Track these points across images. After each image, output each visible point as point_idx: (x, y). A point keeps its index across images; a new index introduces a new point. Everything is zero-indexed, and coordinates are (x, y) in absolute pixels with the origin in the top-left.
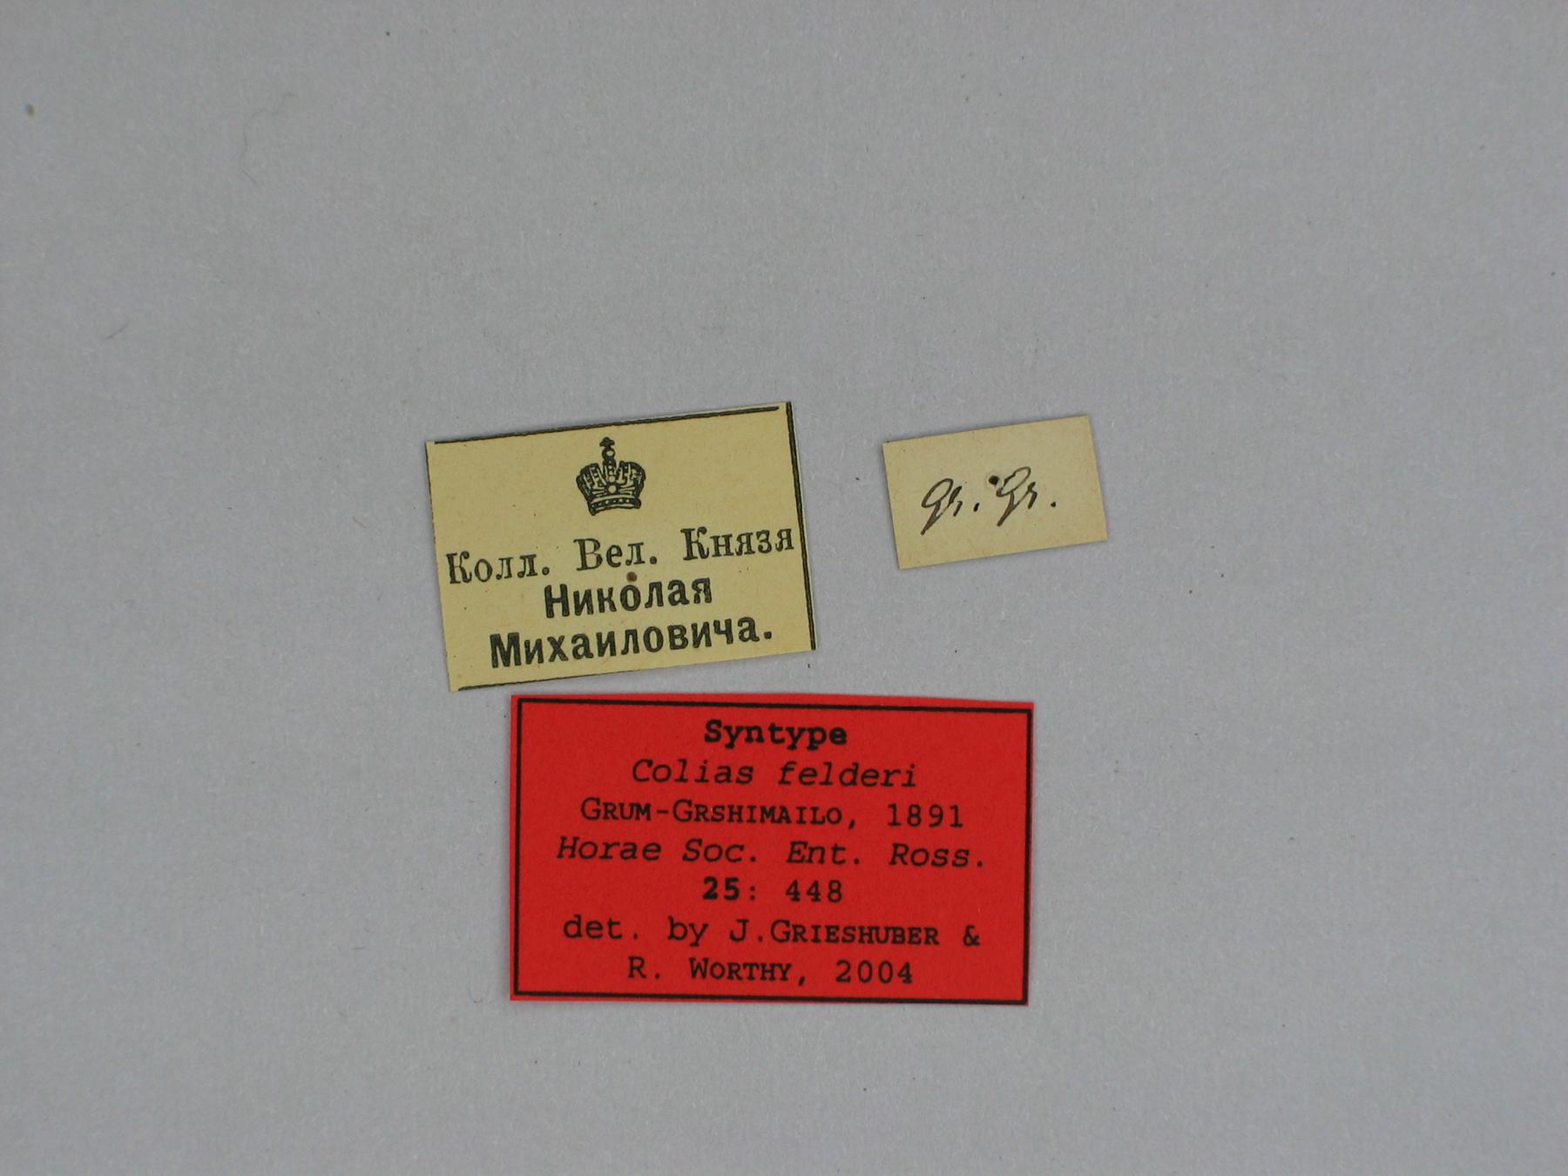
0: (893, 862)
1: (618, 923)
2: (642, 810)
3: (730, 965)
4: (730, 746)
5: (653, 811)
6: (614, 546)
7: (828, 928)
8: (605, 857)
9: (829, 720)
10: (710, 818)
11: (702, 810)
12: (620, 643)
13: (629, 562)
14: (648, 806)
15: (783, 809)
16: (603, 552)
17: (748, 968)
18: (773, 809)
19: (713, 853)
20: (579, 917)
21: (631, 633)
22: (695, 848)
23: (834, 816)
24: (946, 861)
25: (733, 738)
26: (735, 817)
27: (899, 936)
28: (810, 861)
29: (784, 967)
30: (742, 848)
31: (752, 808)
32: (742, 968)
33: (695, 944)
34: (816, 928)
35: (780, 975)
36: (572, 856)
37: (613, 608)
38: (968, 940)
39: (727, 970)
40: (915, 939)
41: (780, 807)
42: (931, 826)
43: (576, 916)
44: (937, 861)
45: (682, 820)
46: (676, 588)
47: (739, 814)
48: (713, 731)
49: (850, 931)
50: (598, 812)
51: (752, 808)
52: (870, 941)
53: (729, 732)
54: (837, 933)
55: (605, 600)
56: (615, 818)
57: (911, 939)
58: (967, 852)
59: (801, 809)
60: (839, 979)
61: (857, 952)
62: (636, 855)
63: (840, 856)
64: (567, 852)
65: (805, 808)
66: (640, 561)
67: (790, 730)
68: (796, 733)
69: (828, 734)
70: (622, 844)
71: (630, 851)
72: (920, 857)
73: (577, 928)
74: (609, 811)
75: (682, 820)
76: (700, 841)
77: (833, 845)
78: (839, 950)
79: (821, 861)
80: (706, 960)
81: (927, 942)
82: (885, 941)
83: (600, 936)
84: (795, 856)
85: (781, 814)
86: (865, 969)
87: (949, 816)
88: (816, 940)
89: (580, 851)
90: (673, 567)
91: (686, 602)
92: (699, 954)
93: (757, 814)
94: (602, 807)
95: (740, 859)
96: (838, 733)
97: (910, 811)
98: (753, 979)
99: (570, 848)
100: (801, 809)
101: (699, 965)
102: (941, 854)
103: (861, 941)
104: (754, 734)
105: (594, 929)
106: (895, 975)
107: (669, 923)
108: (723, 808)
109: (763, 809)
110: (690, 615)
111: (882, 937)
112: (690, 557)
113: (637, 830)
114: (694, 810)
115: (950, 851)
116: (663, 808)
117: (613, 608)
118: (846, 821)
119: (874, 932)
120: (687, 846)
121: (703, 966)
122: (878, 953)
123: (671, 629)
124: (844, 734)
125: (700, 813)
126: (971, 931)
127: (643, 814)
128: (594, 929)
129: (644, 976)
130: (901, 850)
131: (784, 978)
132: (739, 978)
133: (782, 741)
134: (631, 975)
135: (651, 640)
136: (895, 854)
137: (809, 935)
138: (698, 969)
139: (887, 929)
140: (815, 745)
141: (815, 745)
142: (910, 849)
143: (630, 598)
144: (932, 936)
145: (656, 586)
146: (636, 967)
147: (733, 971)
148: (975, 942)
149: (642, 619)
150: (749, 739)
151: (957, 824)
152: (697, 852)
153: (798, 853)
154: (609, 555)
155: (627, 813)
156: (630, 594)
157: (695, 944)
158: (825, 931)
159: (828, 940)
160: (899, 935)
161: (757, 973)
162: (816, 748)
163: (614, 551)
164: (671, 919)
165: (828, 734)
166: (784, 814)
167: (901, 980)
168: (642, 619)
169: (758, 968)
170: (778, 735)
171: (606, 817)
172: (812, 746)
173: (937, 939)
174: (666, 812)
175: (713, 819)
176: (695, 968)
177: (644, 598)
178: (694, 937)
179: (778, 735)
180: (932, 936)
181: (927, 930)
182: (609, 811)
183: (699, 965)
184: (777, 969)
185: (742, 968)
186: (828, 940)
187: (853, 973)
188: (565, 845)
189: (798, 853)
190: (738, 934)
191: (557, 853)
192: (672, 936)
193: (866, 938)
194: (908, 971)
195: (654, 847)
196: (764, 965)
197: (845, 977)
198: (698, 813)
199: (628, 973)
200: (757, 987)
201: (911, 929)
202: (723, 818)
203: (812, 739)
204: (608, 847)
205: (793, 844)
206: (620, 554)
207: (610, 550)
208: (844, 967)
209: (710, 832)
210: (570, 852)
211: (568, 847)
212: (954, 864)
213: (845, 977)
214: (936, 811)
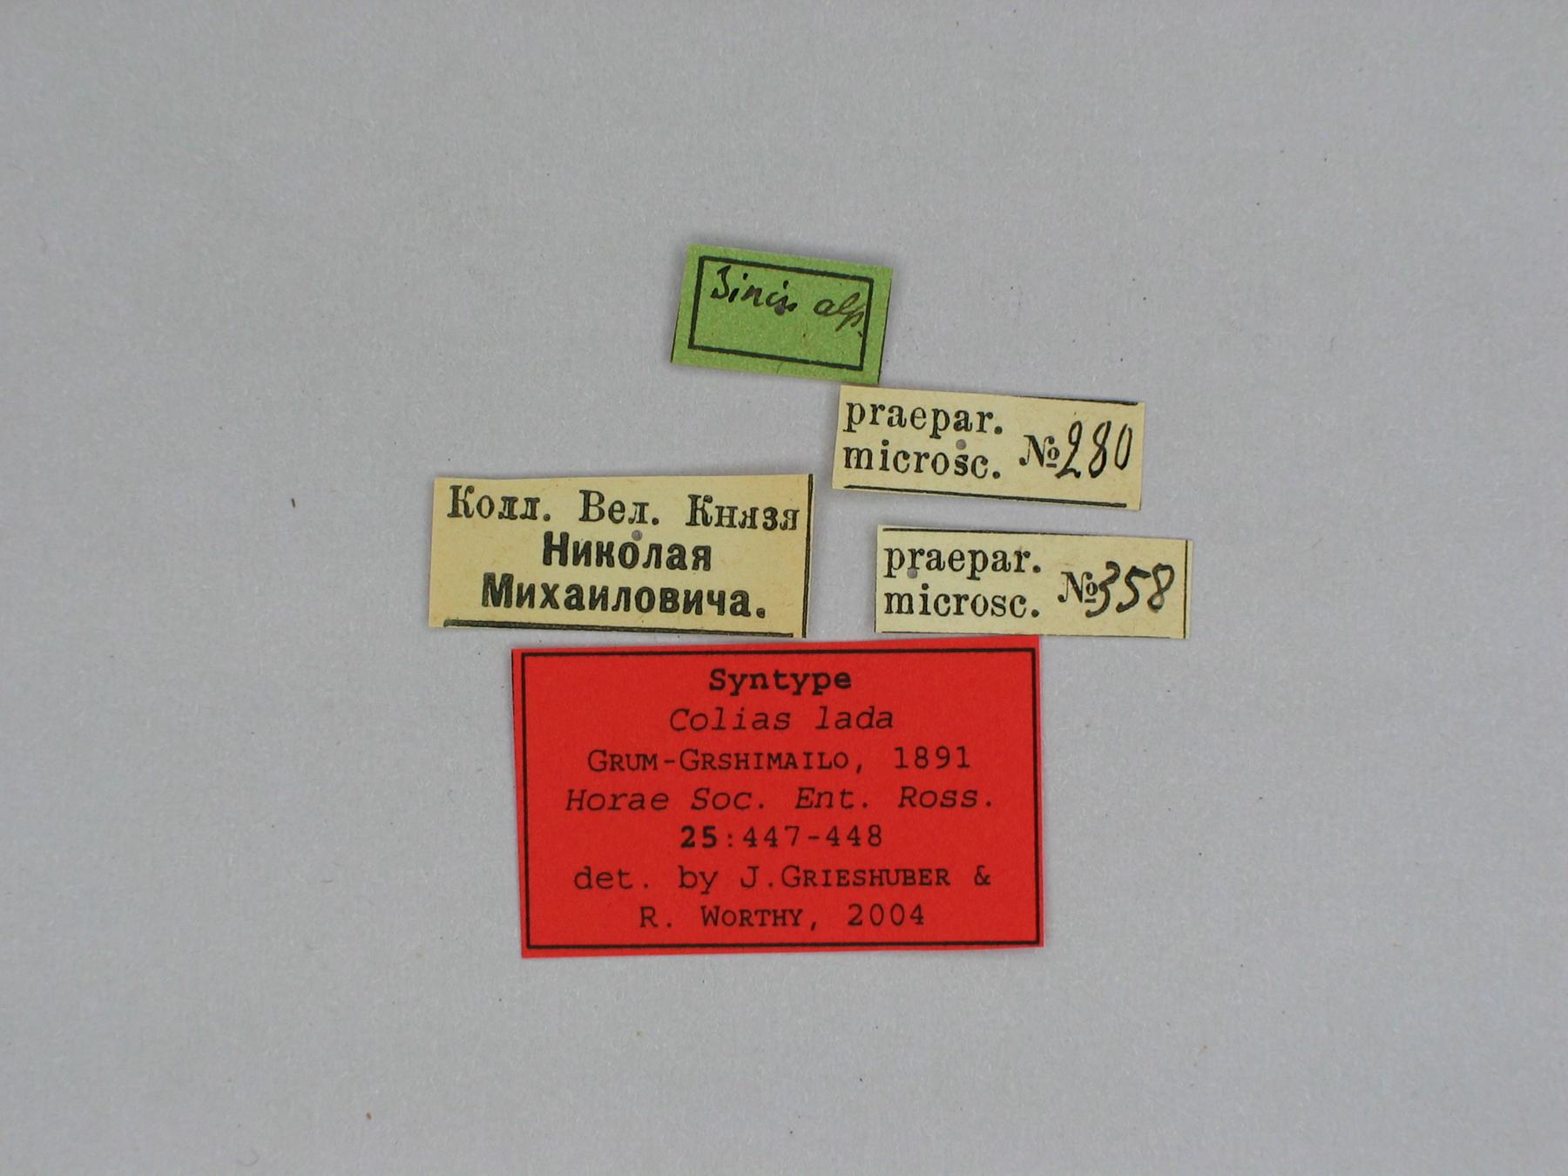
0: (902, 805)
2: (647, 761)
3: (742, 912)
4: (735, 693)
8: (614, 808)
9: (832, 666)
11: (708, 758)
13: (631, 521)
14: (654, 756)
15: (790, 755)
16: (606, 506)
17: (759, 914)
18: (779, 755)
19: (721, 801)
20: (588, 868)
22: (701, 797)
23: (839, 762)
24: (955, 802)
25: (738, 687)
26: (742, 765)
27: (909, 878)
28: (818, 806)
29: (796, 913)
31: (758, 755)
32: (753, 913)
33: (706, 892)
34: (826, 872)
36: (580, 808)
38: (979, 880)
41: (787, 754)
42: (939, 767)
43: (586, 867)
44: (945, 802)
47: (746, 761)
48: (717, 680)
50: (605, 763)
51: (758, 755)
52: (881, 884)
53: (734, 681)
54: (847, 877)
55: (605, 554)
57: (922, 880)
58: (975, 793)
59: (808, 755)
60: (851, 923)
61: (867, 896)
63: (848, 800)
64: (575, 805)
66: (642, 520)
67: (795, 676)
68: (800, 679)
69: (832, 679)
72: (928, 799)
73: (590, 879)
74: (615, 763)
75: (688, 769)
76: (708, 790)
77: (841, 790)
78: (853, 894)
79: (830, 806)
80: (717, 908)
81: (938, 883)
83: (610, 887)
85: (789, 759)
87: (956, 758)
88: (827, 884)
89: (589, 805)
92: (710, 904)
93: (764, 761)
94: (608, 759)
95: (748, 807)
96: (841, 677)
97: (917, 754)
99: (577, 800)
100: (808, 755)
101: (710, 913)
102: (951, 795)
104: (759, 681)
106: (907, 915)
107: (679, 871)
108: (730, 756)
109: (770, 756)
111: (893, 878)
114: (699, 758)
116: (670, 758)
118: (853, 765)
119: (884, 874)
120: (696, 797)
121: (715, 916)
122: (885, 896)
124: (848, 679)
125: (707, 762)
126: (981, 869)
127: (650, 763)
129: (656, 926)
130: (909, 793)
131: (796, 924)
133: (787, 687)
134: (643, 925)
136: (903, 797)
137: (820, 878)
138: (710, 917)
140: (820, 690)
141: (820, 690)
142: (918, 791)
144: (942, 877)
145: (656, 548)
146: (647, 915)
147: (745, 919)
148: (985, 882)
150: (754, 686)
152: (705, 801)
153: (805, 799)
154: (612, 510)
155: (634, 763)
157: (706, 892)
159: (839, 884)
160: (908, 878)
161: (769, 919)
162: (821, 693)
163: (617, 507)
164: (681, 867)
165: (832, 679)
166: (791, 761)
169: (769, 914)
170: (782, 681)
172: (817, 691)
173: (947, 879)
174: (673, 761)
175: (720, 768)
176: (706, 916)
177: (643, 558)
178: (707, 886)
179: (782, 681)
180: (942, 877)
182: (615, 763)
183: (710, 913)
184: (790, 919)
185: (753, 913)
186: (839, 884)
187: (865, 915)
188: (573, 797)
189: (805, 799)
190: (748, 881)
191: (566, 806)
192: (683, 885)
193: (876, 881)
195: (663, 798)
196: (775, 911)
197: (856, 922)
198: (705, 762)
199: (640, 922)
200: (771, 933)
201: (921, 871)
203: (817, 686)
204: (615, 798)
205: (801, 790)
206: (623, 510)
207: (612, 506)
208: (855, 911)
212: (963, 805)
213: (856, 922)
214: (943, 753)
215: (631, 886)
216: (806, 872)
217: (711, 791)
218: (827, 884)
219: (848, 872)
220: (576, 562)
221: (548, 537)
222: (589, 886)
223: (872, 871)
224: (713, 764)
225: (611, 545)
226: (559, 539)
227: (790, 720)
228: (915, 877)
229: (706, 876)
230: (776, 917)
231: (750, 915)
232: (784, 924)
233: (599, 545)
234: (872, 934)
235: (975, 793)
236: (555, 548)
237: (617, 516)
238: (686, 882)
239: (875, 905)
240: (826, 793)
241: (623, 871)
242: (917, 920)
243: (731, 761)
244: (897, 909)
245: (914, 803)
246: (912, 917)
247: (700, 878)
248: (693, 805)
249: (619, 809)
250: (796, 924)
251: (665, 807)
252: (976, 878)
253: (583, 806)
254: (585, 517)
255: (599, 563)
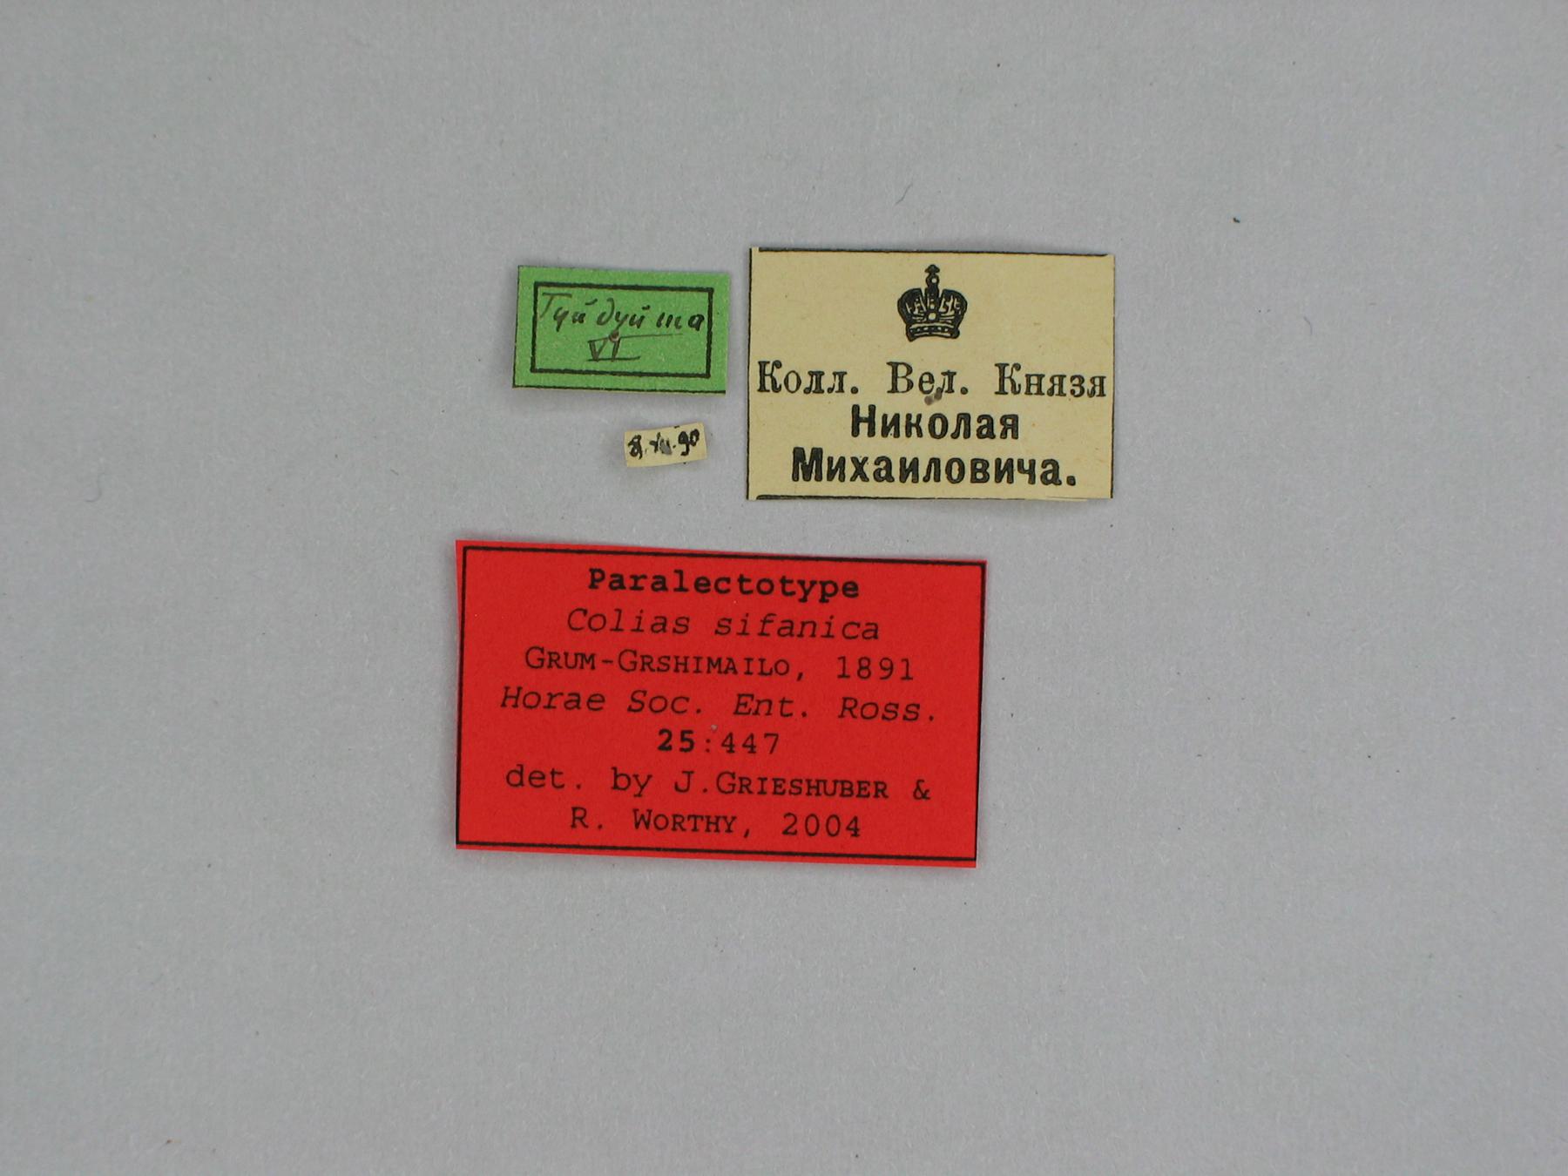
0: (842, 716)
1: (560, 773)
2: (587, 659)
3: (675, 816)
5: (598, 662)
6: (926, 373)
7: (775, 780)
10: (656, 669)
11: (646, 660)
12: (922, 472)
14: (592, 656)
15: (730, 660)
16: (915, 377)
17: (692, 819)
18: (719, 660)
19: (658, 704)
20: (522, 766)
21: (935, 462)
23: (779, 668)
24: (896, 715)
26: (681, 668)
27: (847, 789)
28: (756, 713)
29: (729, 820)
30: (687, 700)
31: (698, 659)
32: (686, 819)
33: (639, 795)
35: (726, 827)
36: (516, 706)
37: (920, 434)
38: (919, 795)
39: (671, 822)
40: (863, 793)
41: (728, 659)
42: (882, 678)
43: (518, 765)
45: (628, 671)
46: (984, 422)
47: (686, 664)
49: (795, 783)
50: (542, 660)
51: (698, 659)
54: (783, 787)
55: (913, 426)
56: (559, 667)
57: (859, 792)
59: (749, 660)
60: (786, 832)
61: (803, 805)
62: (581, 704)
64: (510, 702)
65: (752, 659)
70: (566, 694)
71: (574, 702)
72: (869, 711)
73: (521, 777)
74: (553, 660)
76: (645, 693)
77: (781, 699)
79: (769, 714)
80: (650, 811)
81: (876, 796)
82: (833, 794)
83: (543, 785)
84: (742, 709)
85: (729, 665)
86: (812, 822)
87: (900, 670)
88: (762, 792)
90: (983, 400)
91: (993, 437)
93: (703, 665)
94: (546, 656)
95: (685, 711)
98: (697, 830)
99: (513, 698)
100: (749, 660)
101: (642, 816)
103: (809, 794)
105: (537, 778)
106: (843, 827)
107: (613, 771)
109: (710, 660)
110: (994, 450)
111: (830, 789)
112: (1002, 391)
113: (582, 682)
115: (900, 706)
117: (920, 434)
118: (793, 675)
119: (822, 784)
121: (646, 819)
122: (824, 806)
123: (974, 462)
125: (646, 662)
126: (921, 785)
127: (588, 662)
128: (537, 778)
129: (586, 826)
131: (729, 831)
132: (683, 830)
134: (574, 826)
135: (954, 470)
136: (844, 708)
137: (755, 787)
139: (835, 782)
143: (938, 427)
144: (881, 790)
145: (964, 418)
146: (579, 817)
147: (677, 823)
149: (946, 449)
151: (907, 677)
152: (643, 704)
153: (743, 705)
154: (921, 382)
155: (571, 662)
156: (938, 423)
157: (639, 795)
158: (773, 783)
159: (775, 793)
160: (846, 789)
161: (702, 825)
163: (926, 378)
164: (615, 769)
167: (848, 834)
168: (946, 449)
171: (550, 666)
173: (886, 792)
175: (659, 670)
176: (638, 819)
177: (952, 428)
178: (639, 789)
181: (876, 784)
182: (553, 660)
183: (642, 816)
184: (722, 825)
185: (686, 819)
186: (775, 793)
187: (800, 825)
188: (509, 694)
189: (743, 705)
190: (682, 785)
193: (814, 791)
194: (856, 823)
195: (598, 698)
196: (708, 817)
197: (789, 831)
200: (704, 839)
201: (859, 783)
202: (669, 666)
204: (551, 696)
205: (740, 696)
206: (932, 380)
207: (921, 379)
209: (653, 682)
210: (514, 700)
211: (511, 697)
214: (886, 664)
215: (562, 786)
216: (741, 779)
217: (647, 696)
218: (762, 792)
219: (784, 781)
220: (885, 433)
221: (856, 409)
222: (521, 783)
223: (809, 781)
224: (651, 665)
225: (919, 417)
226: (867, 411)
227: (731, 626)
228: (854, 788)
229: (639, 778)
230: (708, 823)
231: (683, 820)
232: (717, 830)
233: (909, 416)
234: (810, 844)
235: (918, 707)
236: (861, 421)
237: (927, 387)
238: (618, 784)
239: (831, 816)
240: (765, 700)
241: (556, 770)
242: (853, 832)
243: (669, 663)
244: (833, 820)
245: (854, 713)
246: (848, 828)
247: (633, 780)
248: (630, 707)
249: (554, 707)
250: (729, 831)
251: (601, 708)
252: (915, 793)
253: (519, 704)
254: (894, 390)
255: (908, 434)
